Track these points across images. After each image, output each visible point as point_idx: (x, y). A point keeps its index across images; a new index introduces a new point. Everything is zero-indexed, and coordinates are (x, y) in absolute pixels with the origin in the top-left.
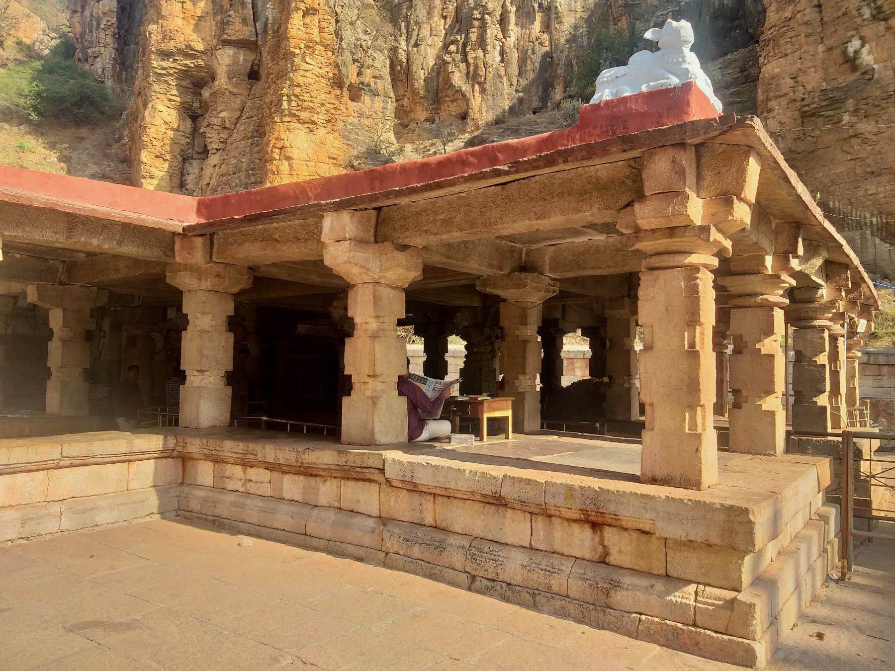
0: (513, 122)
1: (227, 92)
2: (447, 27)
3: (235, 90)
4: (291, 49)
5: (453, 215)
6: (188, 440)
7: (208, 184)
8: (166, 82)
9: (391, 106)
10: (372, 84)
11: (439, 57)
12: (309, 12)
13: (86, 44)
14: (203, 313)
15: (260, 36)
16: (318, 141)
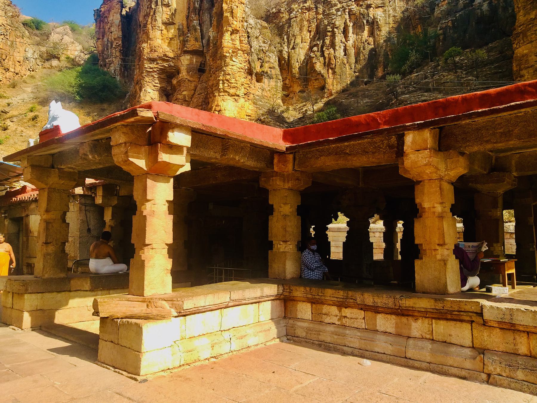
0: (353, 90)
1: (187, 80)
2: (311, 37)
3: (191, 79)
5: (511, 128)
6: (293, 288)
8: (152, 76)
9: (280, 84)
10: (269, 72)
11: (307, 55)
12: (235, 32)
13: (105, 56)
14: (285, 204)
16: (240, 106)
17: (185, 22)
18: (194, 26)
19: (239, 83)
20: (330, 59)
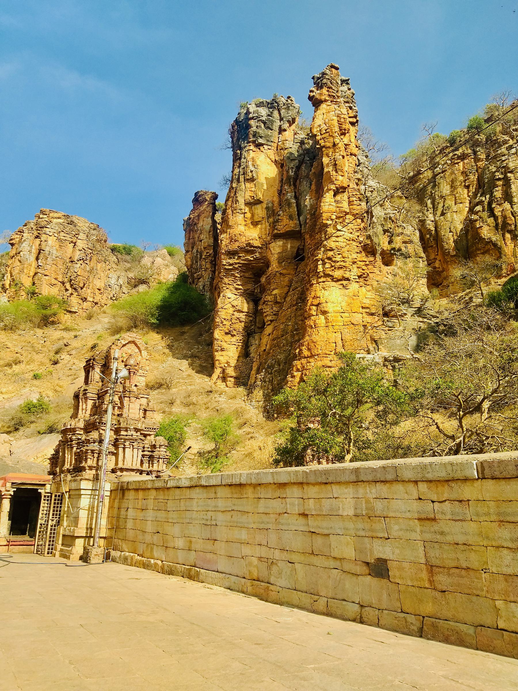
3: (284, 272)
4: (324, 222)
7: (265, 350)
8: (233, 275)
10: (403, 249)
12: (339, 190)
15: (303, 226)
16: (351, 294)
17: (276, 199)
18: (287, 200)
19: (349, 261)
20: (505, 217)
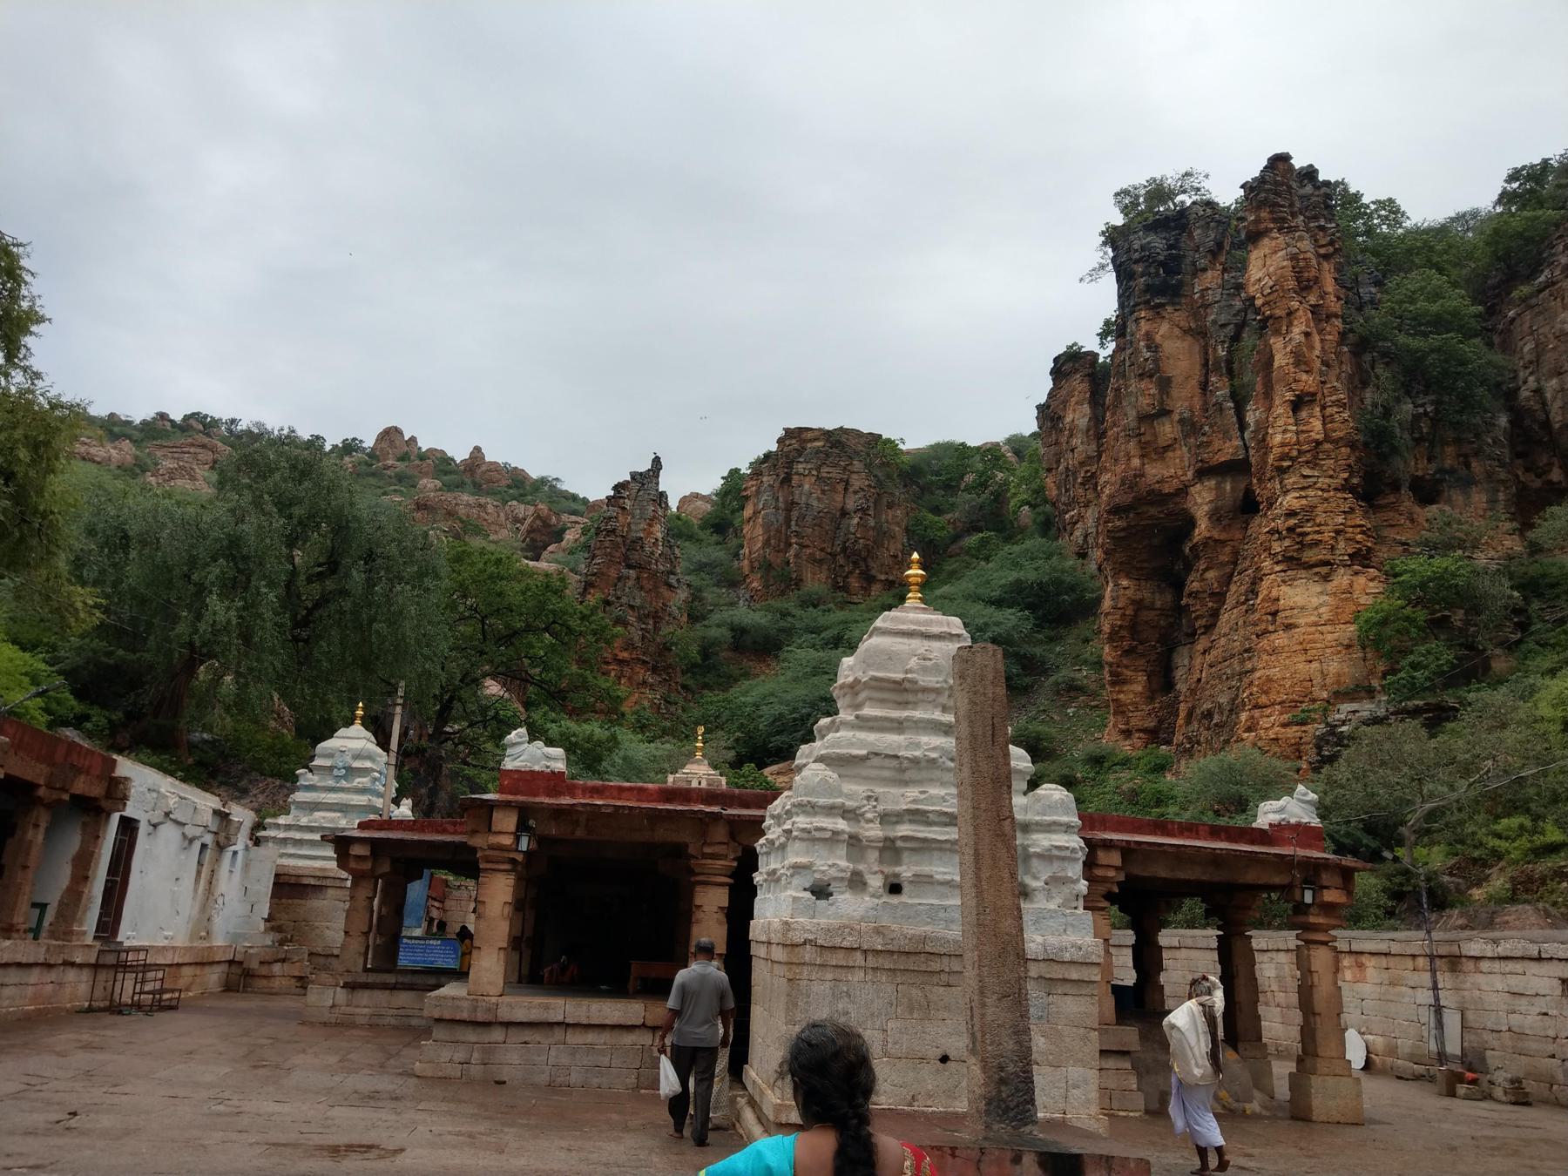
7: (1199, 680)
